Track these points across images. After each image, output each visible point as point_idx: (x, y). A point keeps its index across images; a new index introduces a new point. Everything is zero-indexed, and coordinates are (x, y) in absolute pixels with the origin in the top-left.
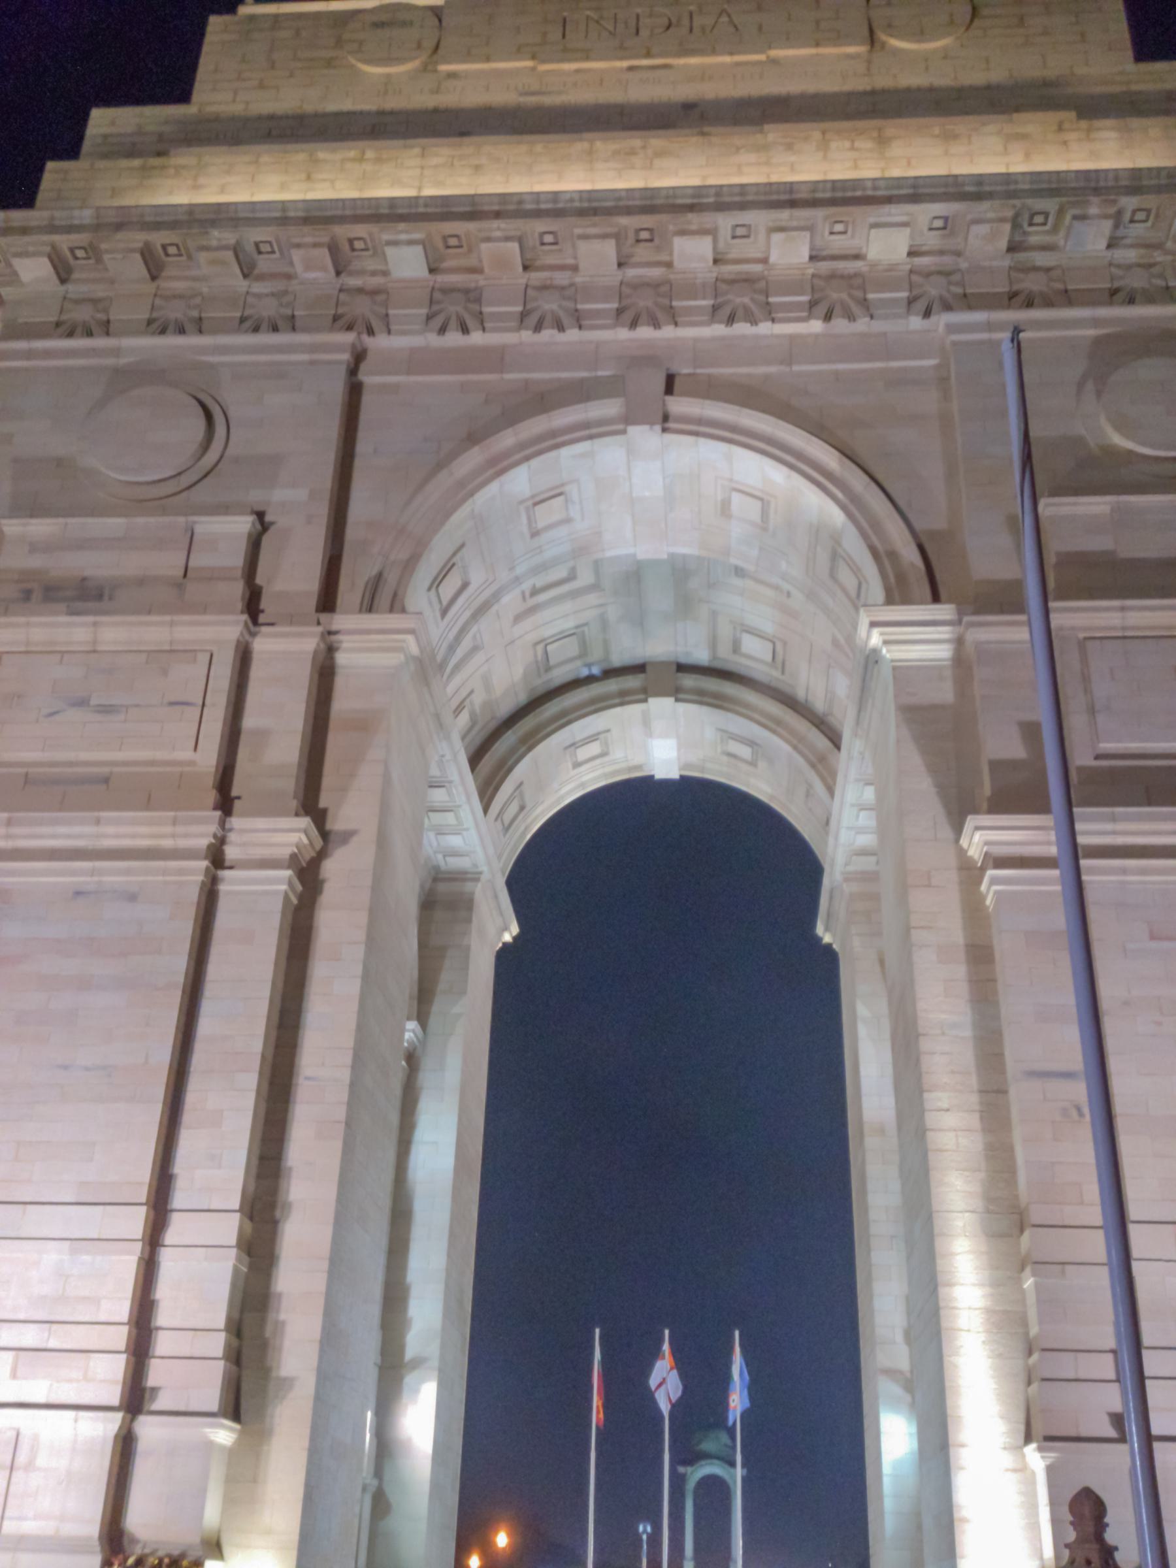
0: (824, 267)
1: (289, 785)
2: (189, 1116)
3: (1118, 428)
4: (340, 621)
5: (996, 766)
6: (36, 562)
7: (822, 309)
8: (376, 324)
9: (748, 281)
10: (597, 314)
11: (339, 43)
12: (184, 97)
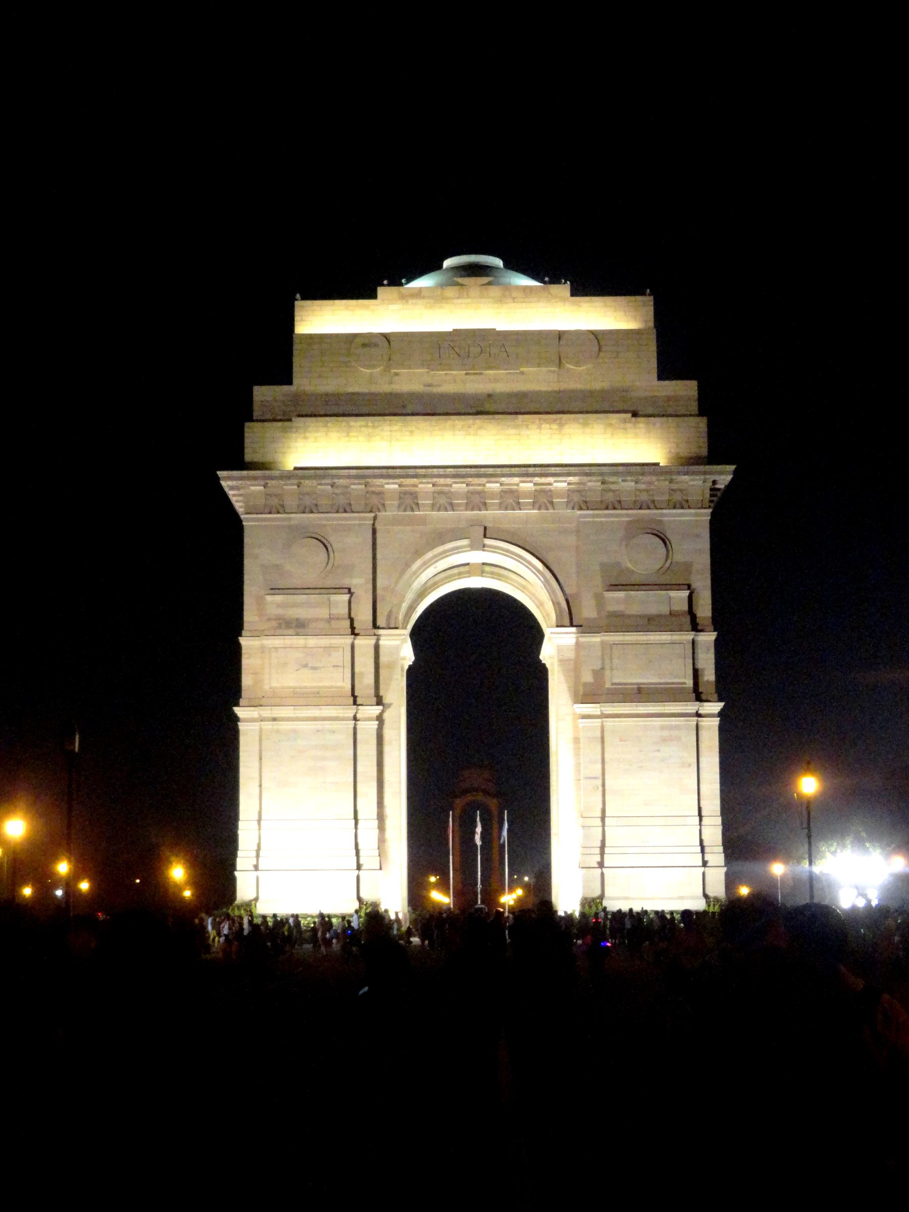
0: (538, 487)
1: (372, 692)
2: (358, 795)
3: (630, 561)
4: (381, 632)
5: (585, 684)
6: (280, 611)
7: (537, 506)
8: (381, 507)
9: (511, 492)
10: (459, 505)
11: (349, 354)
12: (290, 383)
